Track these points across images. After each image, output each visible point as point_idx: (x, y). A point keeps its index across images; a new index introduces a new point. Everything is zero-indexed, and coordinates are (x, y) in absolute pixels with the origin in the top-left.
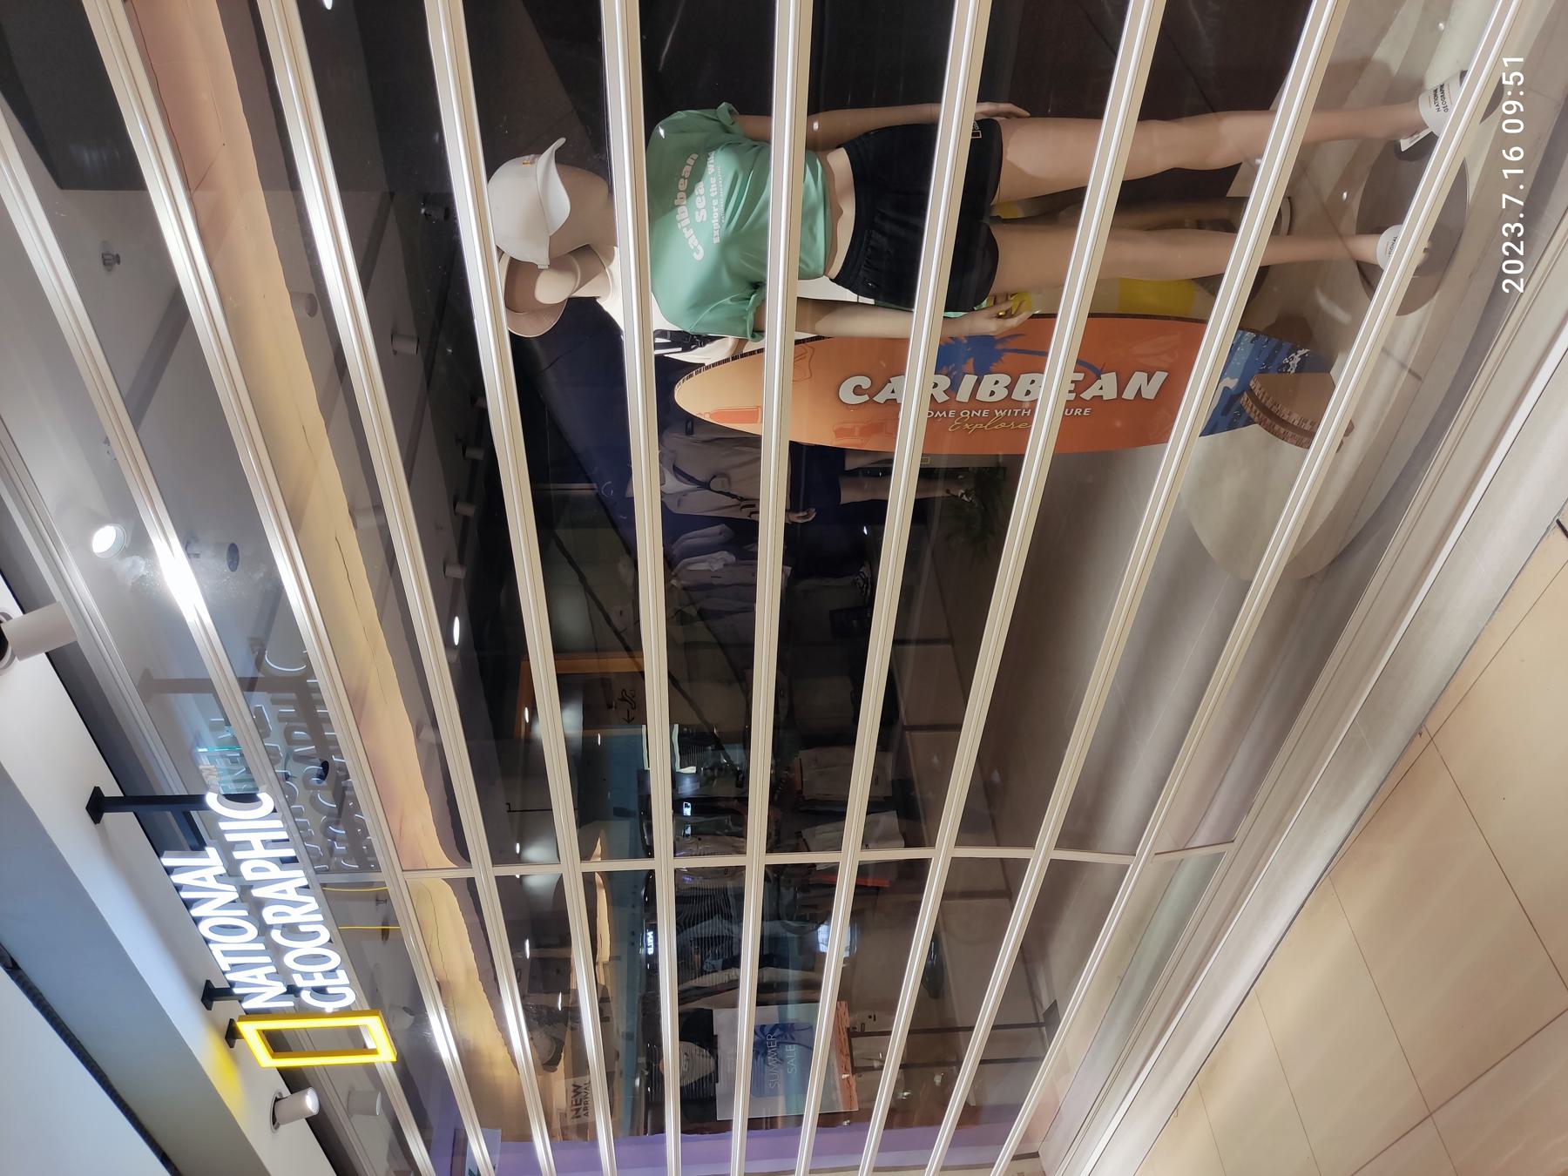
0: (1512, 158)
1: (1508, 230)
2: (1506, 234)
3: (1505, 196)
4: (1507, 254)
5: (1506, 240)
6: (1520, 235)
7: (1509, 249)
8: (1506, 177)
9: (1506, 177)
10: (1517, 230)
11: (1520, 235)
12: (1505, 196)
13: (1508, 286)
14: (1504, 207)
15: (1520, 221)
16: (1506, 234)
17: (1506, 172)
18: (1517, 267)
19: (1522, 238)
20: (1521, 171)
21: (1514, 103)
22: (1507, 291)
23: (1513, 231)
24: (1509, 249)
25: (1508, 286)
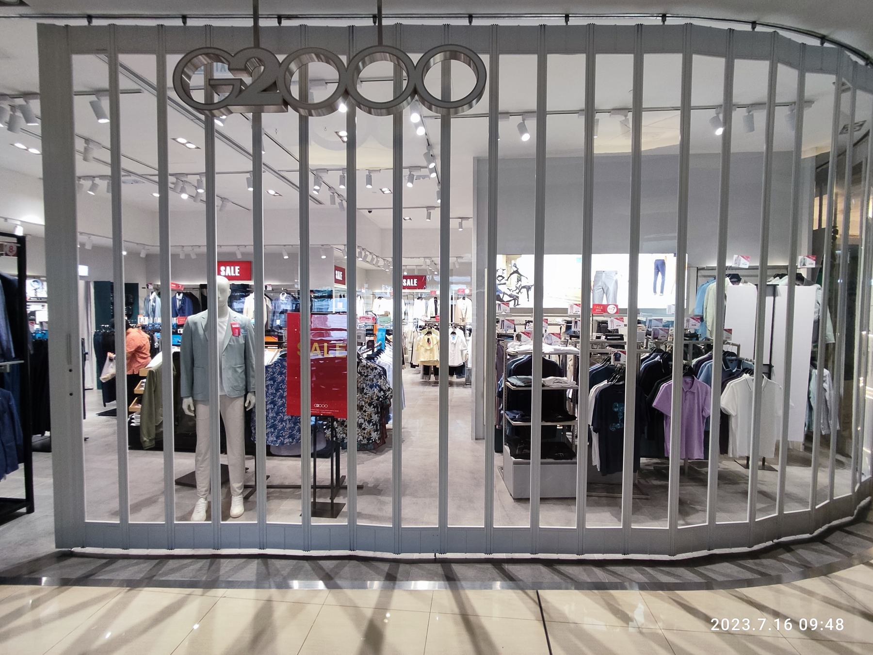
0: (786, 624)
1: (746, 622)
2: (743, 621)
3: (765, 620)
5: (741, 621)
6: (743, 628)
7: (736, 621)
9: (775, 621)
10: (746, 627)
12: (765, 620)
14: (759, 619)
15: (751, 628)
16: (743, 621)
21: (816, 625)
23: (745, 624)
24: (736, 621)
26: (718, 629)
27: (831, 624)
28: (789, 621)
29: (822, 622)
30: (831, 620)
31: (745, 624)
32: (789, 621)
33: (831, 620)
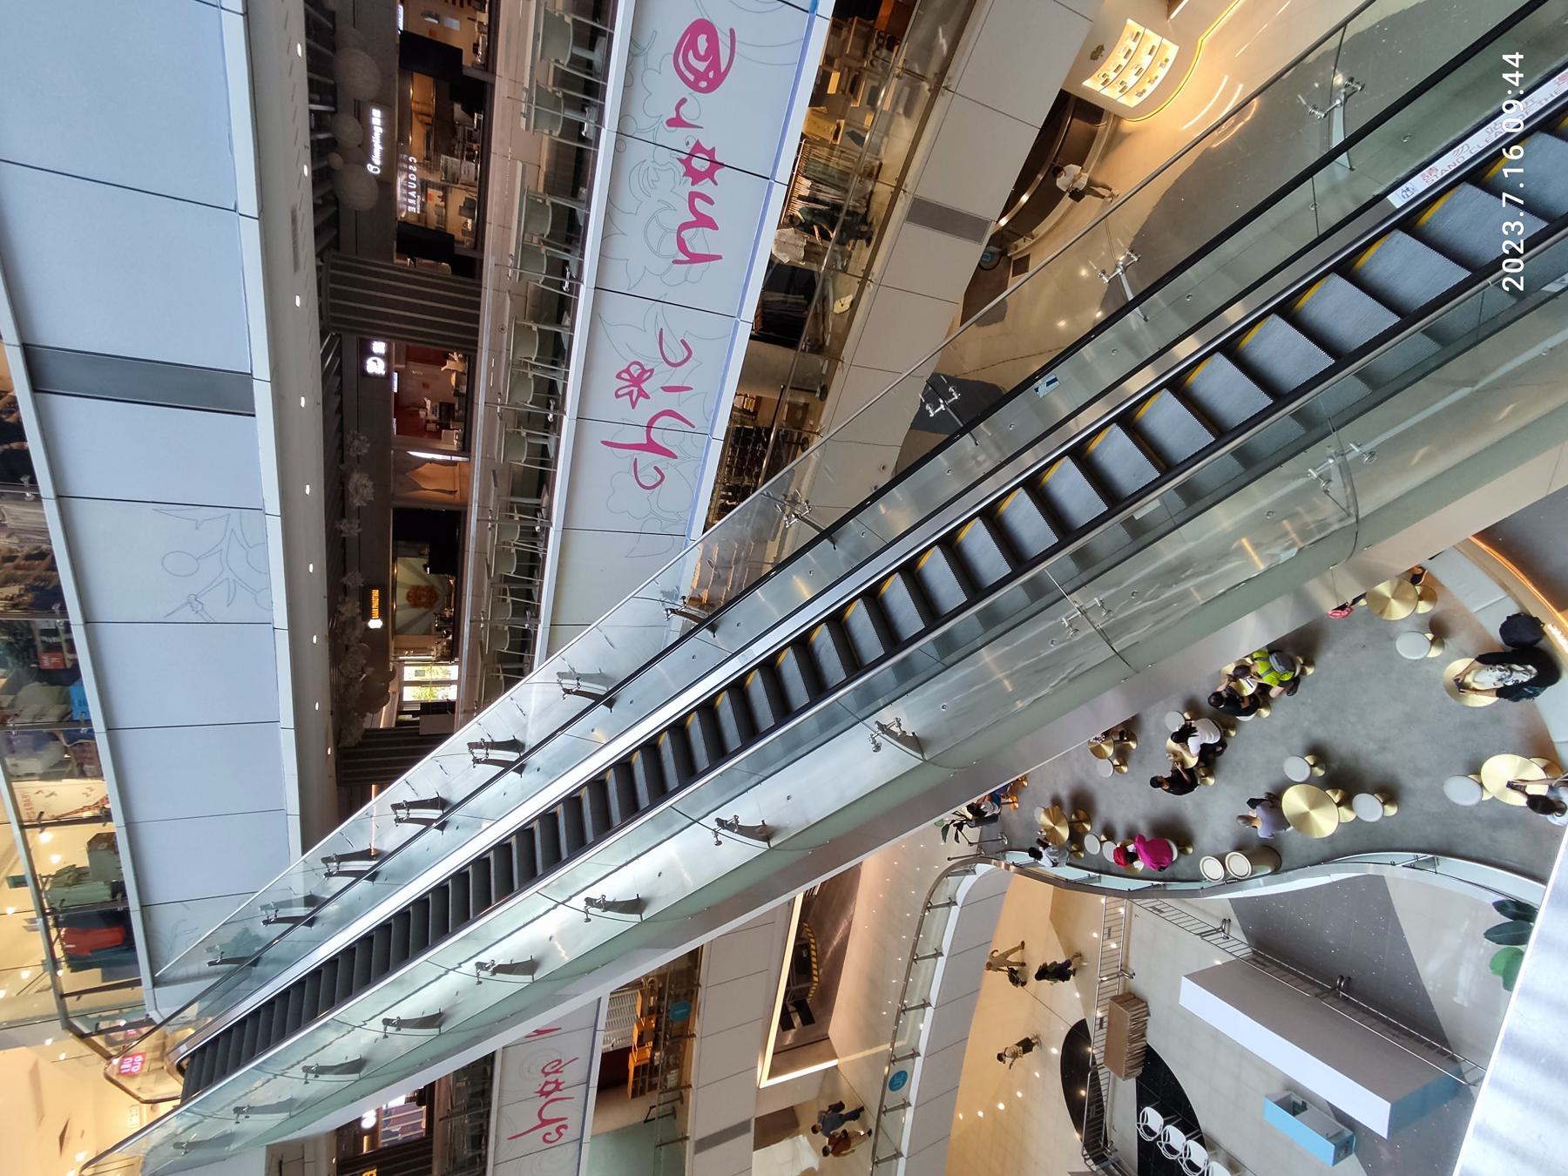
1: (1508, 228)
2: (1506, 233)
4: (1507, 252)
6: (1520, 233)
8: (1506, 176)
9: (1506, 176)
10: (1518, 228)
11: (1520, 233)
13: (1508, 284)
15: (1520, 219)
16: (1506, 233)
17: (1506, 171)
18: (1518, 266)
19: (1521, 236)
20: (1521, 170)
22: (1507, 289)
23: (1513, 229)
25: (1508, 284)
26: (1522, 278)
27: (1512, 75)
28: (1508, 151)
29: (1510, 92)
30: (1506, 76)
31: (1513, 229)
32: (1508, 151)
33: (1506, 76)
